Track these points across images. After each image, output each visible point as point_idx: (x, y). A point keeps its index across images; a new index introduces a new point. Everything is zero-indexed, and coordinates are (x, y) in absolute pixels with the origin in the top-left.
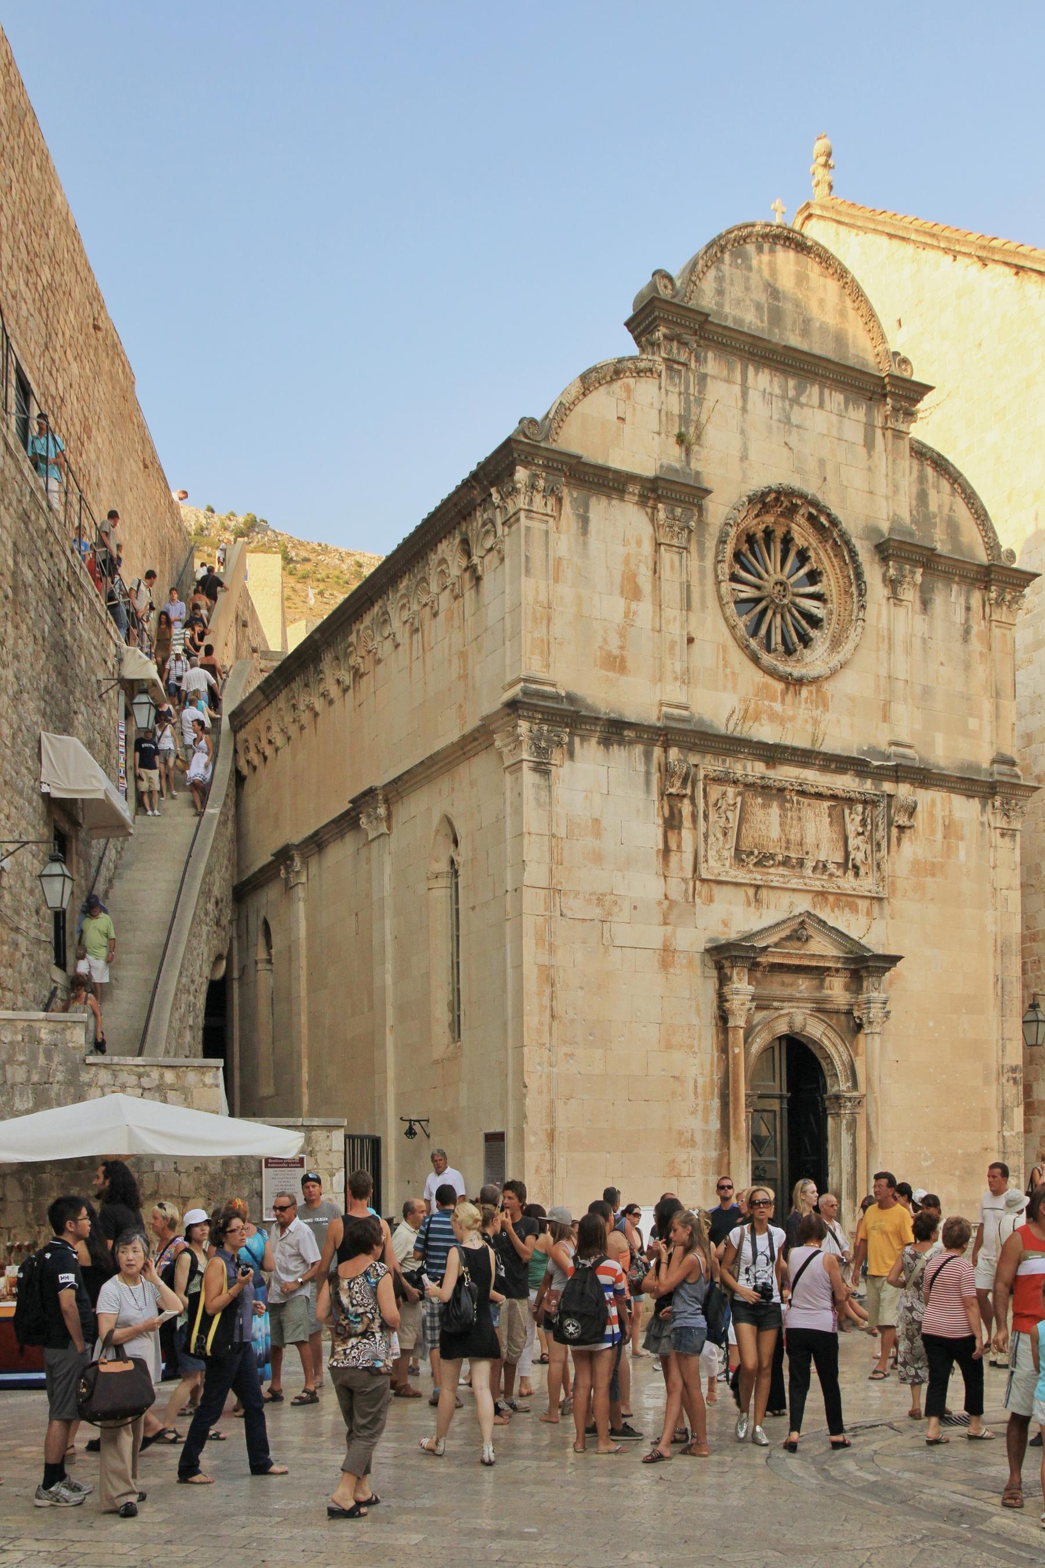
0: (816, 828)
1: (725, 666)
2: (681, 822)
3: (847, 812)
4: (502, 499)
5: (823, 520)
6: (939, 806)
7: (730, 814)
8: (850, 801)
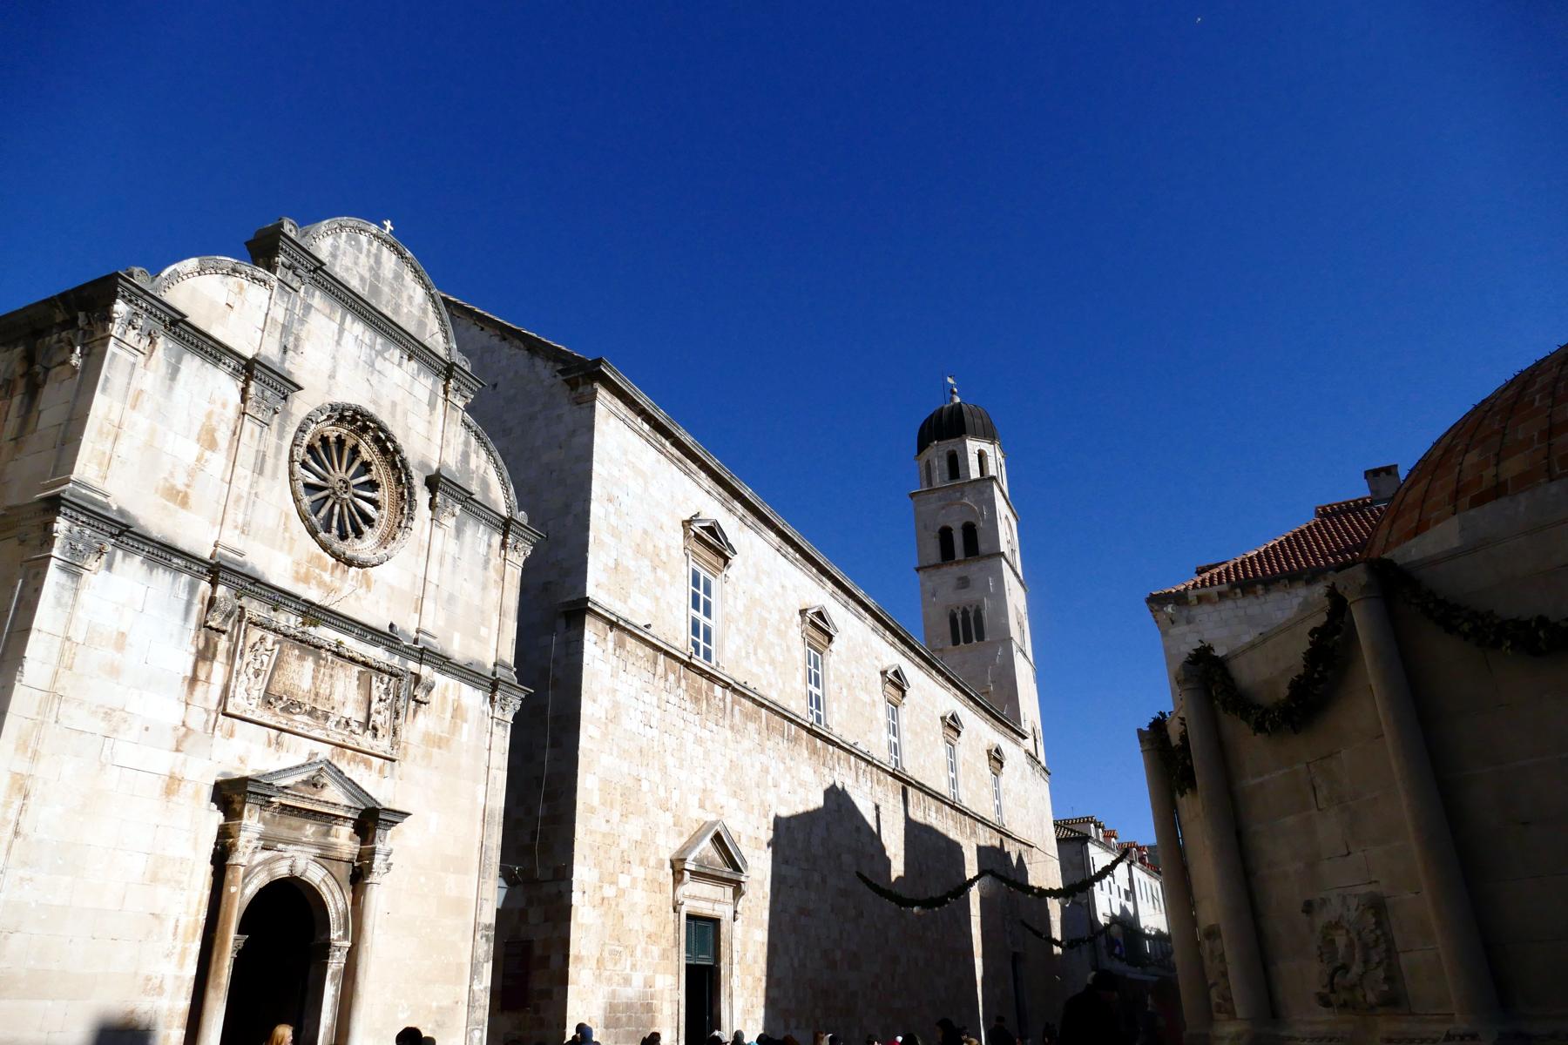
0: (344, 688)
1: (286, 529)
4: (89, 323)
7: (266, 659)
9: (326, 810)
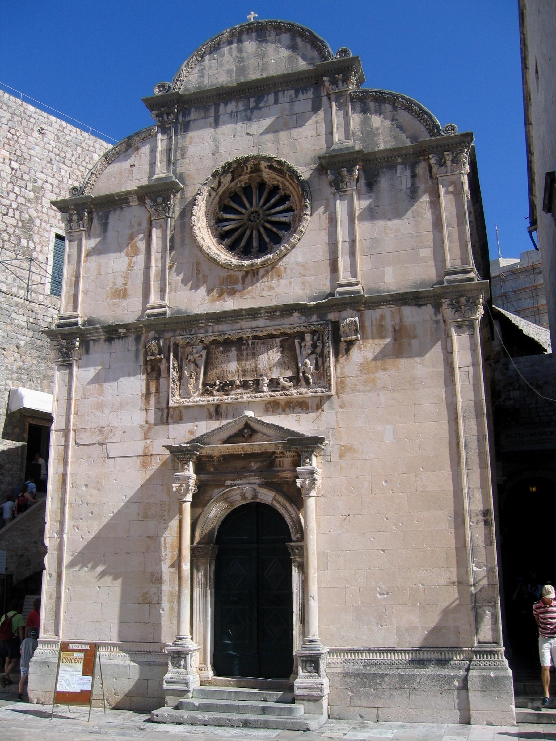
1: (198, 274)
3: (296, 341)
6: (388, 318)
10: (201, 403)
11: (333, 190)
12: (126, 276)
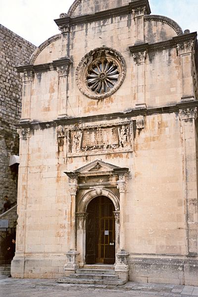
2: (63, 144)
5: (111, 52)
6: (156, 118)
8: (120, 126)
9: (102, 174)
10: (79, 155)
11: (135, 63)
12: (49, 102)
